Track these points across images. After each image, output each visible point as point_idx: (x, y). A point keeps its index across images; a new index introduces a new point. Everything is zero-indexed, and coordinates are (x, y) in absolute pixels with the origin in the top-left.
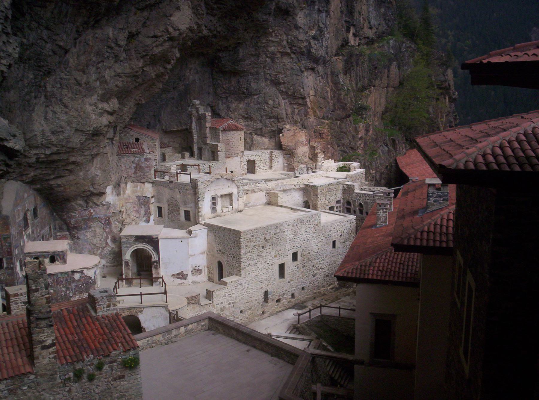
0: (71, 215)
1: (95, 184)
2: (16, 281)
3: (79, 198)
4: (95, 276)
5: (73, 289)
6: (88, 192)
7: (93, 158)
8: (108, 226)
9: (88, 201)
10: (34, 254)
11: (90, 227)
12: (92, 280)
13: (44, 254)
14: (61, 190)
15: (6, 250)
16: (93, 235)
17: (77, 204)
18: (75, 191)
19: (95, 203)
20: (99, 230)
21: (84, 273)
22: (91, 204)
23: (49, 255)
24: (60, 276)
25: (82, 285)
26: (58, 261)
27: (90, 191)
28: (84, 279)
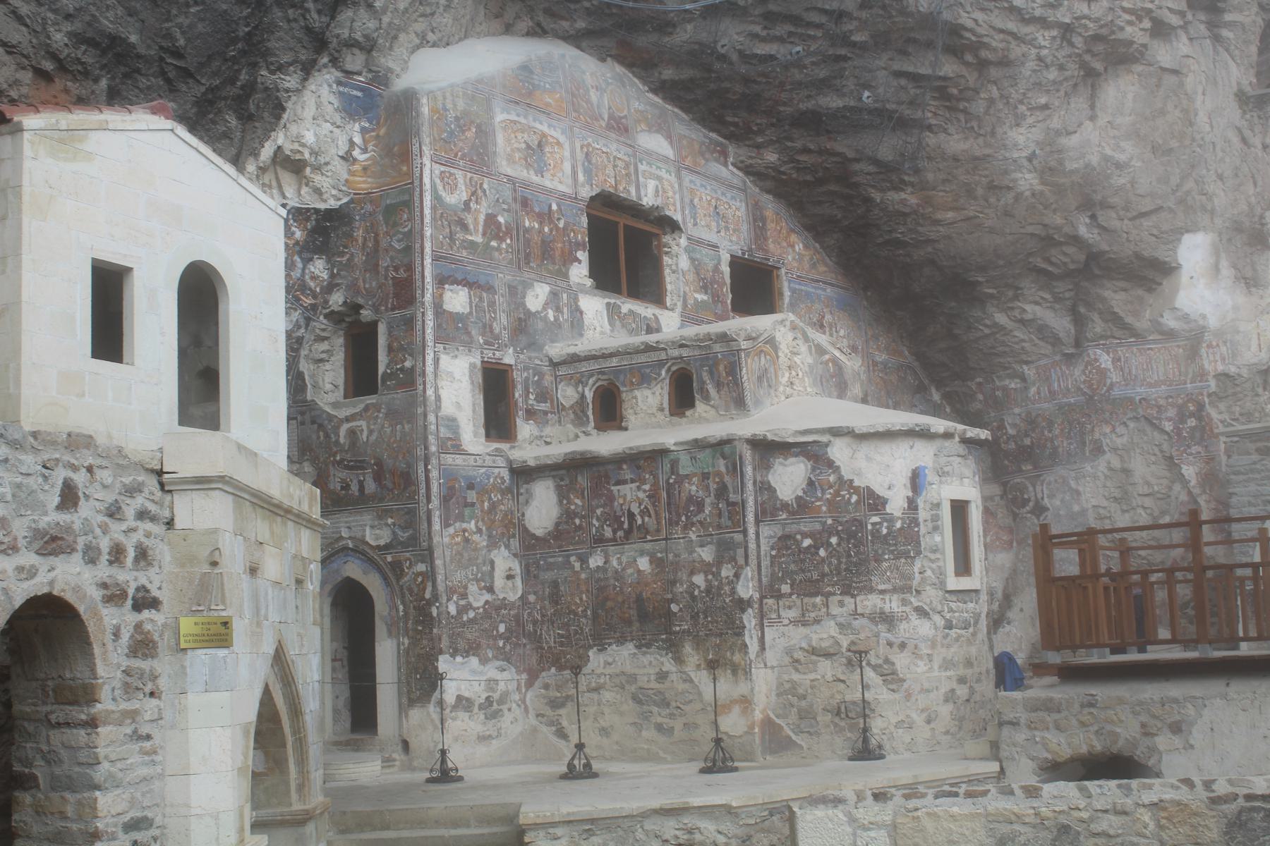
0: (1005, 389)
1: (1105, 205)
2: (420, 452)
3: (1029, 286)
4: (912, 505)
5: (765, 563)
6: (1070, 250)
7: (1090, 75)
8: (1195, 449)
9: (1082, 310)
10: (594, 366)
11: (1098, 450)
12: (891, 520)
13: (642, 358)
14: (903, 202)
15: (392, 273)
16: (1117, 493)
17: (1022, 322)
18: (992, 231)
19: (1115, 319)
20: (1144, 469)
21: (830, 464)
22: (1098, 326)
23: (661, 363)
24: (685, 467)
25: (820, 539)
26: (706, 398)
27: (1076, 240)
28: (829, 503)
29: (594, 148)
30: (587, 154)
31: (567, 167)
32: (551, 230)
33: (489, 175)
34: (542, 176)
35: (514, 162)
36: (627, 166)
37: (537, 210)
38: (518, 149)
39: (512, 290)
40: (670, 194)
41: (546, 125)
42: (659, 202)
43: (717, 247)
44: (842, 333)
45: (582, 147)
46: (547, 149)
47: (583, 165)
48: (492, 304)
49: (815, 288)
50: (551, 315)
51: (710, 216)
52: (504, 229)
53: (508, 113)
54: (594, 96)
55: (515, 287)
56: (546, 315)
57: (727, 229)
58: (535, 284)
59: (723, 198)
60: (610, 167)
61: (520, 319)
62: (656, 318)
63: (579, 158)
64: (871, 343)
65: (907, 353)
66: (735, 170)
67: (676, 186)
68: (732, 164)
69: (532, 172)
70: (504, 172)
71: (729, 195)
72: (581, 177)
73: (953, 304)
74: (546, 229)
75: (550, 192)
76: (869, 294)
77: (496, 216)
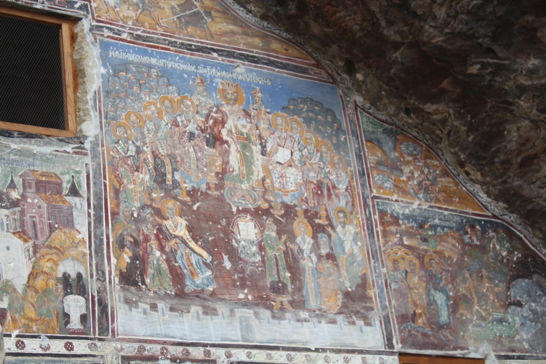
44: (283, 155)
49: (196, 64)
64: (377, 178)
65: (483, 197)
73: (533, 62)
76: (360, 77)
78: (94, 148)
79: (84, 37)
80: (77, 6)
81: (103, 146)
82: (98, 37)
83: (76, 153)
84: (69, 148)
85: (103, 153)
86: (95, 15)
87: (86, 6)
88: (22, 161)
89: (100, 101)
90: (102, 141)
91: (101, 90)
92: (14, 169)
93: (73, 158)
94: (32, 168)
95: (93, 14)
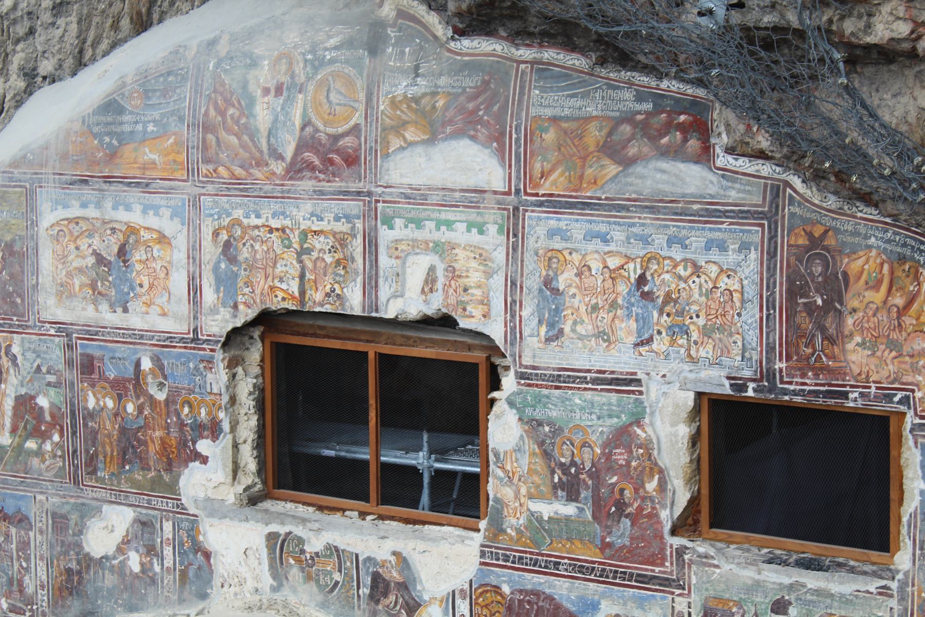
29: (245, 229)
30: (227, 245)
31: (179, 282)
32: (140, 409)
33: (22, 329)
34: (126, 310)
35: (71, 296)
36: (341, 241)
37: (111, 375)
38: (80, 270)
39: (59, 521)
40: (475, 277)
41: (138, 208)
42: (434, 306)
43: (638, 382)
45: (216, 234)
46: (138, 256)
47: (216, 269)
48: (24, 545)
50: (134, 562)
51: (614, 305)
52: (48, 418)
53: (65, 207)
54: (262, 116)
55: (65, 517)
56: (123, 564)
57: (678, 330)
58: (105, 508)
59: (677, 254)
60: (290, 257)
61: (69, 571)
62: (402, 560)
63: (206, 257)
66: (743, 164)
67: (500, 256)
68: (730, 150)
69: (104, 307)
70: (50, 318)
71: (697, 239)
72: (209, 296)
74: (130, 408)
75: (136, 337)
77: (33, 398)
78: (902, 588)
79: (907, 439)
80: (896, 399)
81: (913, 585)
82: (920, 440)
83: (880, 594)
84: (873, 585)
85: (913, 594)
86: (919, 409)
87: (908, 397)
88: (819, 602)
89: (915, 527)
90: (913, 579)
91: (919, 511)
92: (810, 611)
93: (876, 599)
94: (829, 611)
95: (915, 409)
